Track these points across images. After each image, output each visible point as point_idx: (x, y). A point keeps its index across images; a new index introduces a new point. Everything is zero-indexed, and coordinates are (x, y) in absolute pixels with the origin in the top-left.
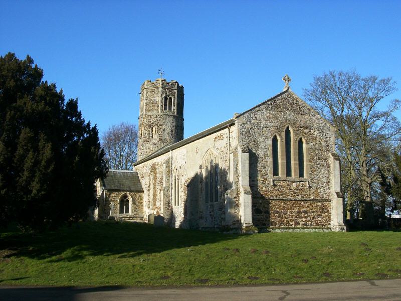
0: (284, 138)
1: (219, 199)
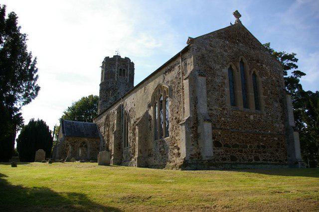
0: (239, 69)
1: (170, 134)
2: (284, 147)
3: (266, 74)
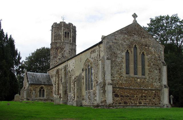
0: (133, 52)
1: (93, 88)
2: (159, 96)
3: (151, 53)
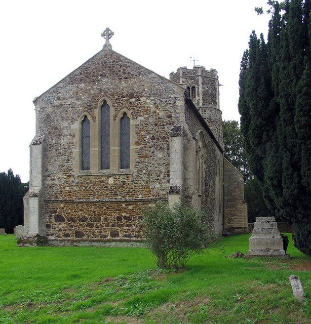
3: (146, 111)
